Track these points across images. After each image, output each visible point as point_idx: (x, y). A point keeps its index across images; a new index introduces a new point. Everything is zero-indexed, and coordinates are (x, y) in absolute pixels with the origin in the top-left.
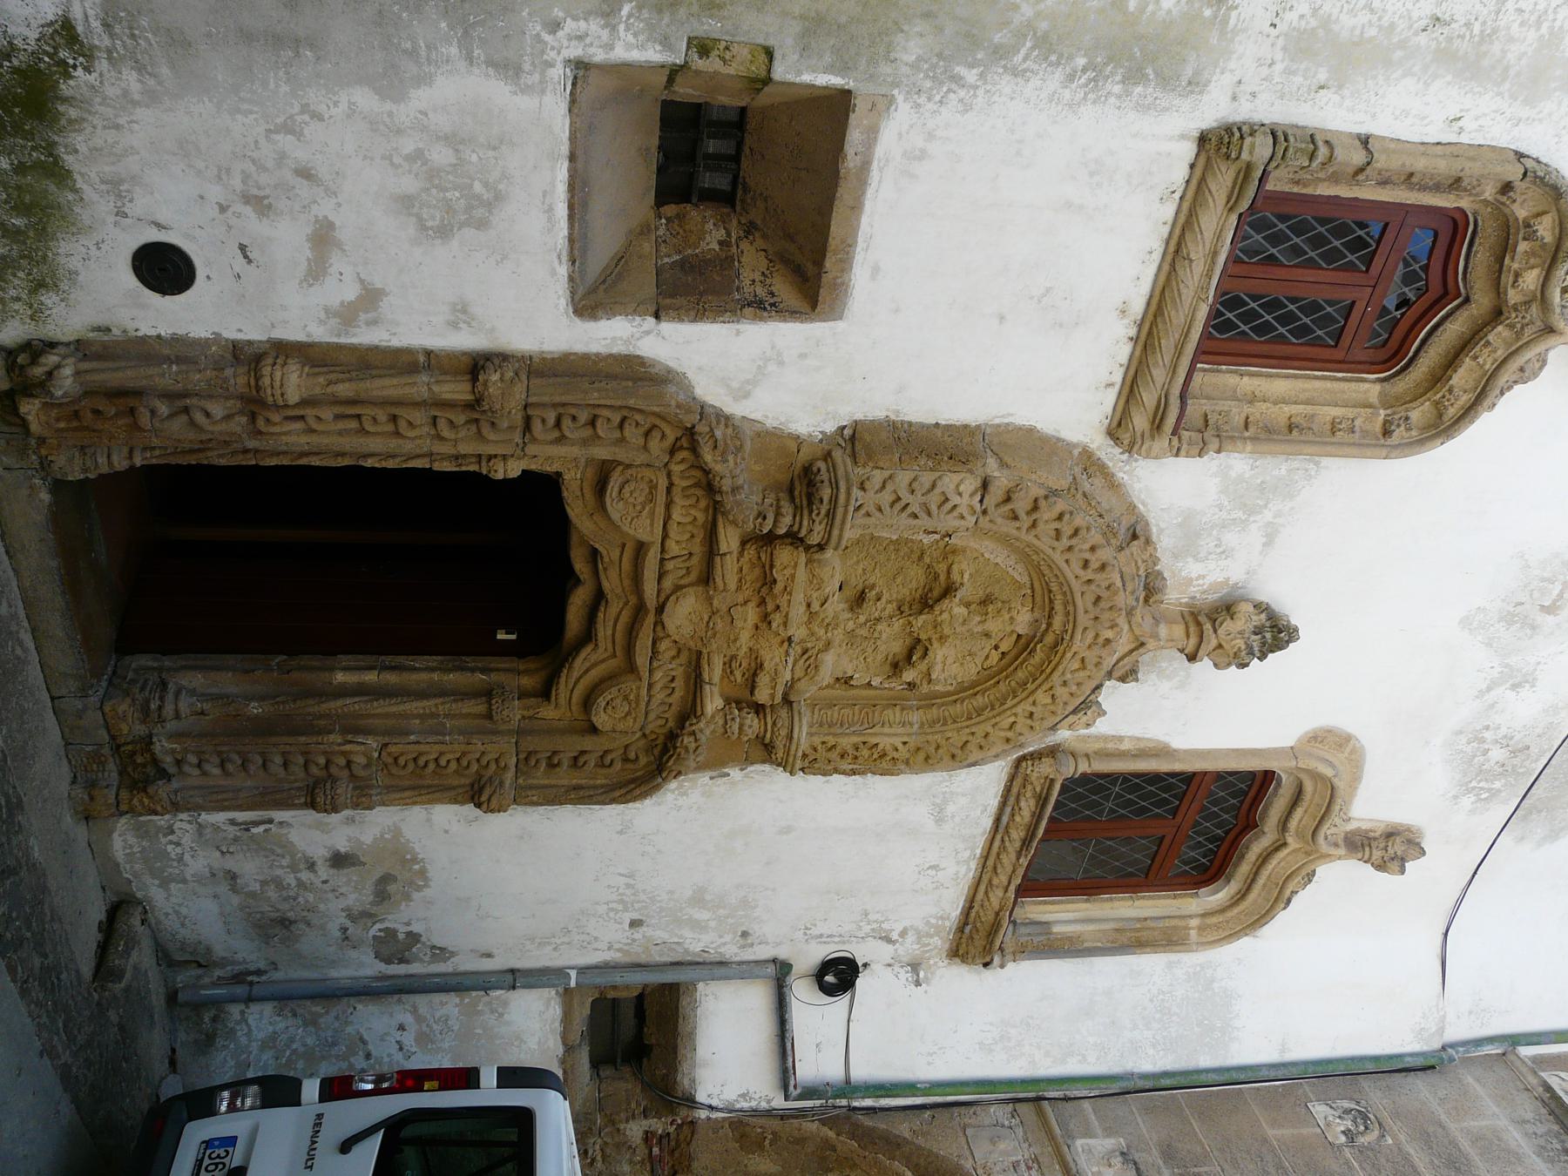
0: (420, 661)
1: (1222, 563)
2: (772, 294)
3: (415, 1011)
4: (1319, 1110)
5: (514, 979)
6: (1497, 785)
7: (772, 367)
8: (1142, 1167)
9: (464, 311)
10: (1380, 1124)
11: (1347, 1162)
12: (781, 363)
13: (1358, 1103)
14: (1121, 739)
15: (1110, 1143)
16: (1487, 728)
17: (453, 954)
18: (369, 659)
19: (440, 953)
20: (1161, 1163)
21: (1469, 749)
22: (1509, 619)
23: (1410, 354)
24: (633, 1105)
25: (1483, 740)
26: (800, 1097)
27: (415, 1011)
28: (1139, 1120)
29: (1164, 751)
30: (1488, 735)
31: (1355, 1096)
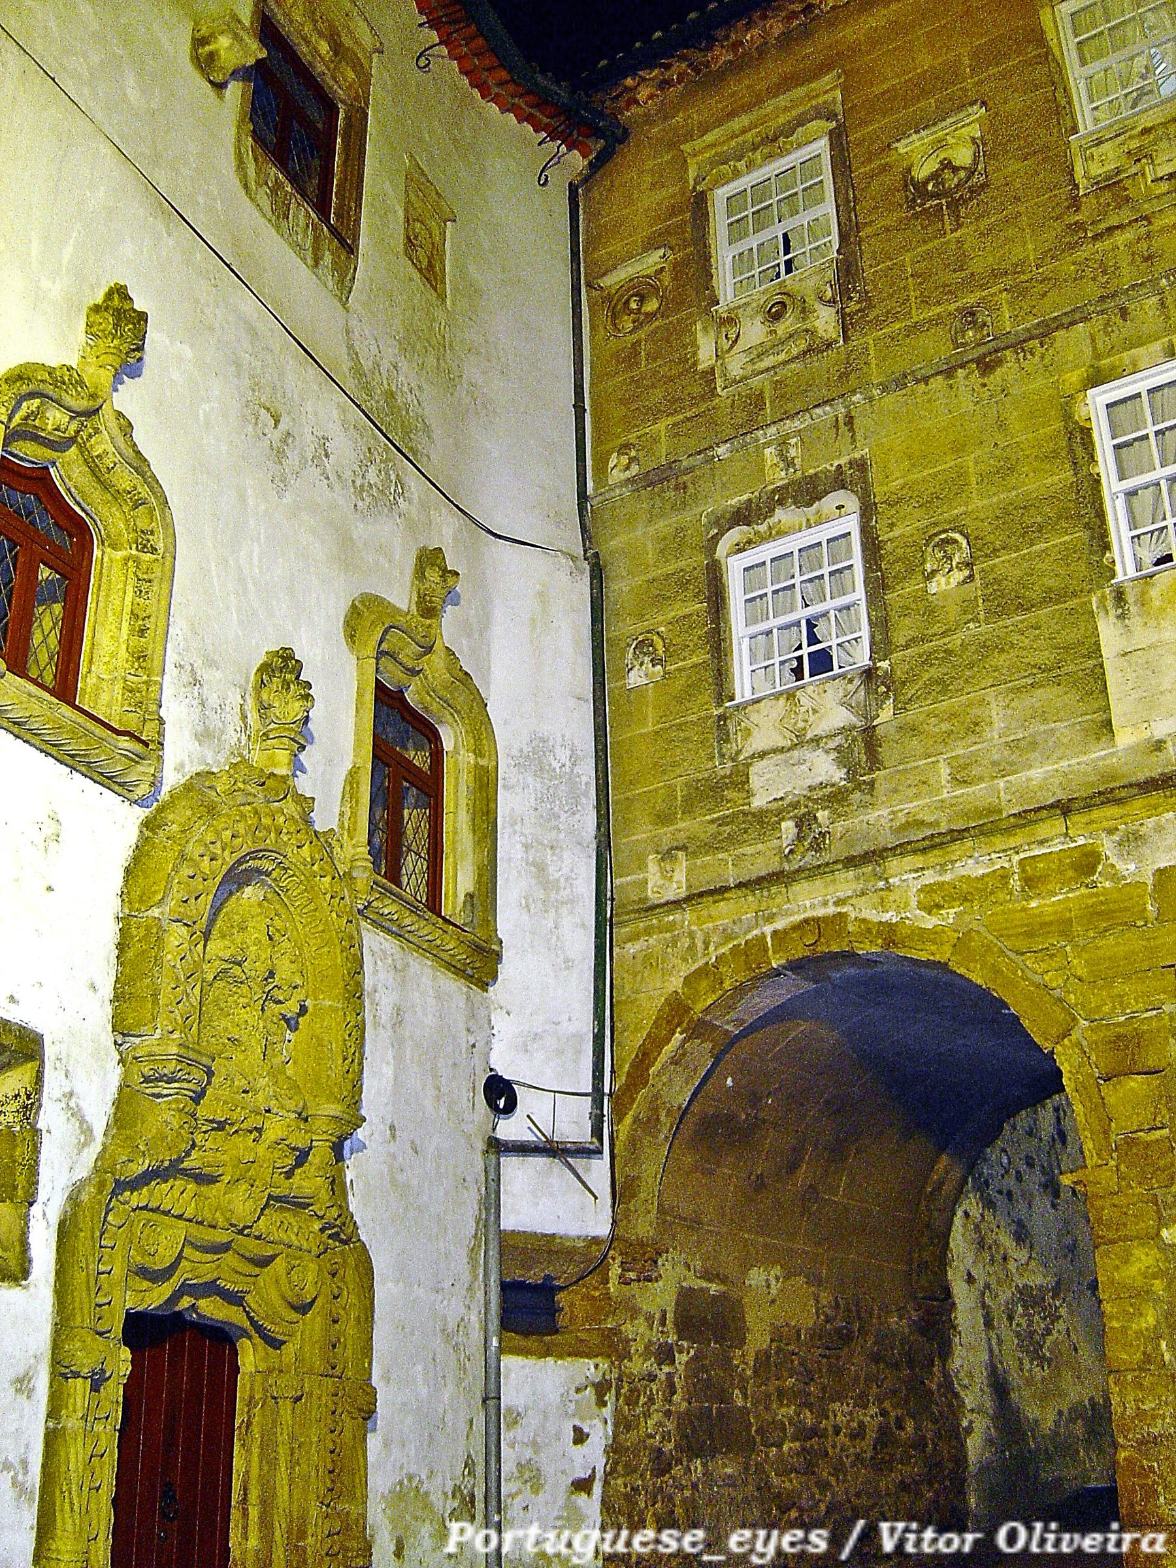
0: (238, 1463)
1: (228, 709)
2: (17, 1096)
3: (512, 1496)
4: (635, 679)
5: (491, 1398)
6: (393, 477)
7: (72, 1104)
8: (675, 844)
9: (20, 1380)
10: (648, 632)
11: (679, 670)
12: (71, 1094)
13: (629, 645)
14: (342, 814)
15: (653, 868)
16: (353, 482)
17: (469, 1456)
18: (235, 1515)
19: (469, 1464)
20: (671, 828)
21: (368, 500)
22: (280, 455)
23: (83, 515)
24: (597, 1294)
25: (362, 486)
26: (601, 1140)
27: (512, 1496)
28: (634, 838)
29: (353, 774)
30: (358, 484)
31: (623, 645)
